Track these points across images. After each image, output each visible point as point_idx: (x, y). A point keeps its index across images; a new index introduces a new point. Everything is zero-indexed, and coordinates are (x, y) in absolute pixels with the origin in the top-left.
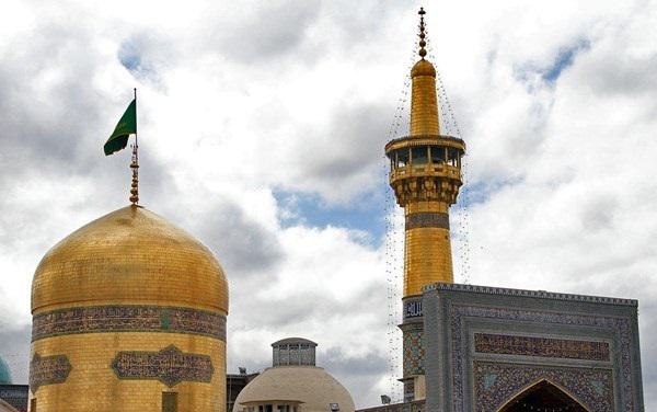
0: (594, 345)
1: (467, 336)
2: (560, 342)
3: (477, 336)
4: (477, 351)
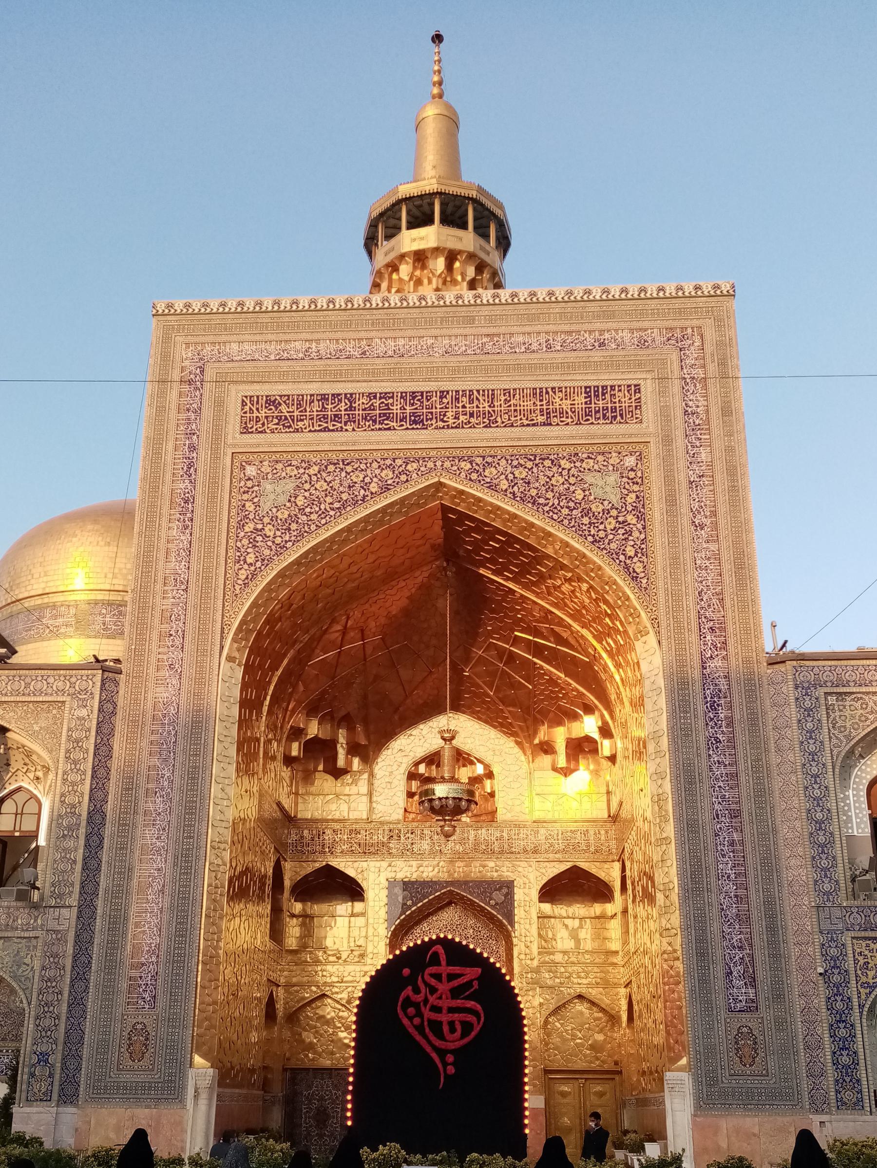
0: (590, 392)
1: (219, 404)
2: (491, 396)
4: (246, 431)
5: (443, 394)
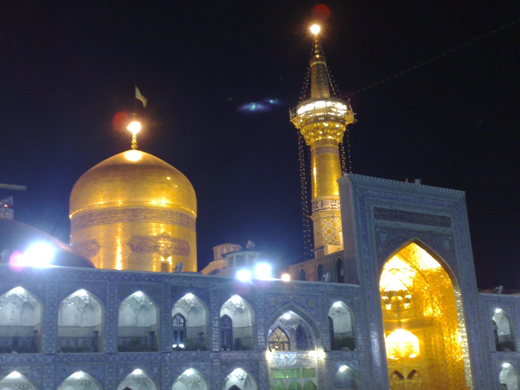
0: (443, 218)
3: (375, 208)
4: (376, 218)
5: (414, 213)
